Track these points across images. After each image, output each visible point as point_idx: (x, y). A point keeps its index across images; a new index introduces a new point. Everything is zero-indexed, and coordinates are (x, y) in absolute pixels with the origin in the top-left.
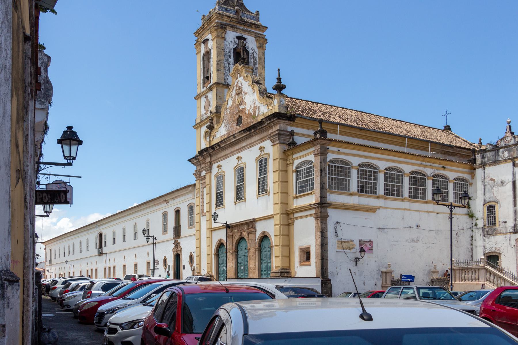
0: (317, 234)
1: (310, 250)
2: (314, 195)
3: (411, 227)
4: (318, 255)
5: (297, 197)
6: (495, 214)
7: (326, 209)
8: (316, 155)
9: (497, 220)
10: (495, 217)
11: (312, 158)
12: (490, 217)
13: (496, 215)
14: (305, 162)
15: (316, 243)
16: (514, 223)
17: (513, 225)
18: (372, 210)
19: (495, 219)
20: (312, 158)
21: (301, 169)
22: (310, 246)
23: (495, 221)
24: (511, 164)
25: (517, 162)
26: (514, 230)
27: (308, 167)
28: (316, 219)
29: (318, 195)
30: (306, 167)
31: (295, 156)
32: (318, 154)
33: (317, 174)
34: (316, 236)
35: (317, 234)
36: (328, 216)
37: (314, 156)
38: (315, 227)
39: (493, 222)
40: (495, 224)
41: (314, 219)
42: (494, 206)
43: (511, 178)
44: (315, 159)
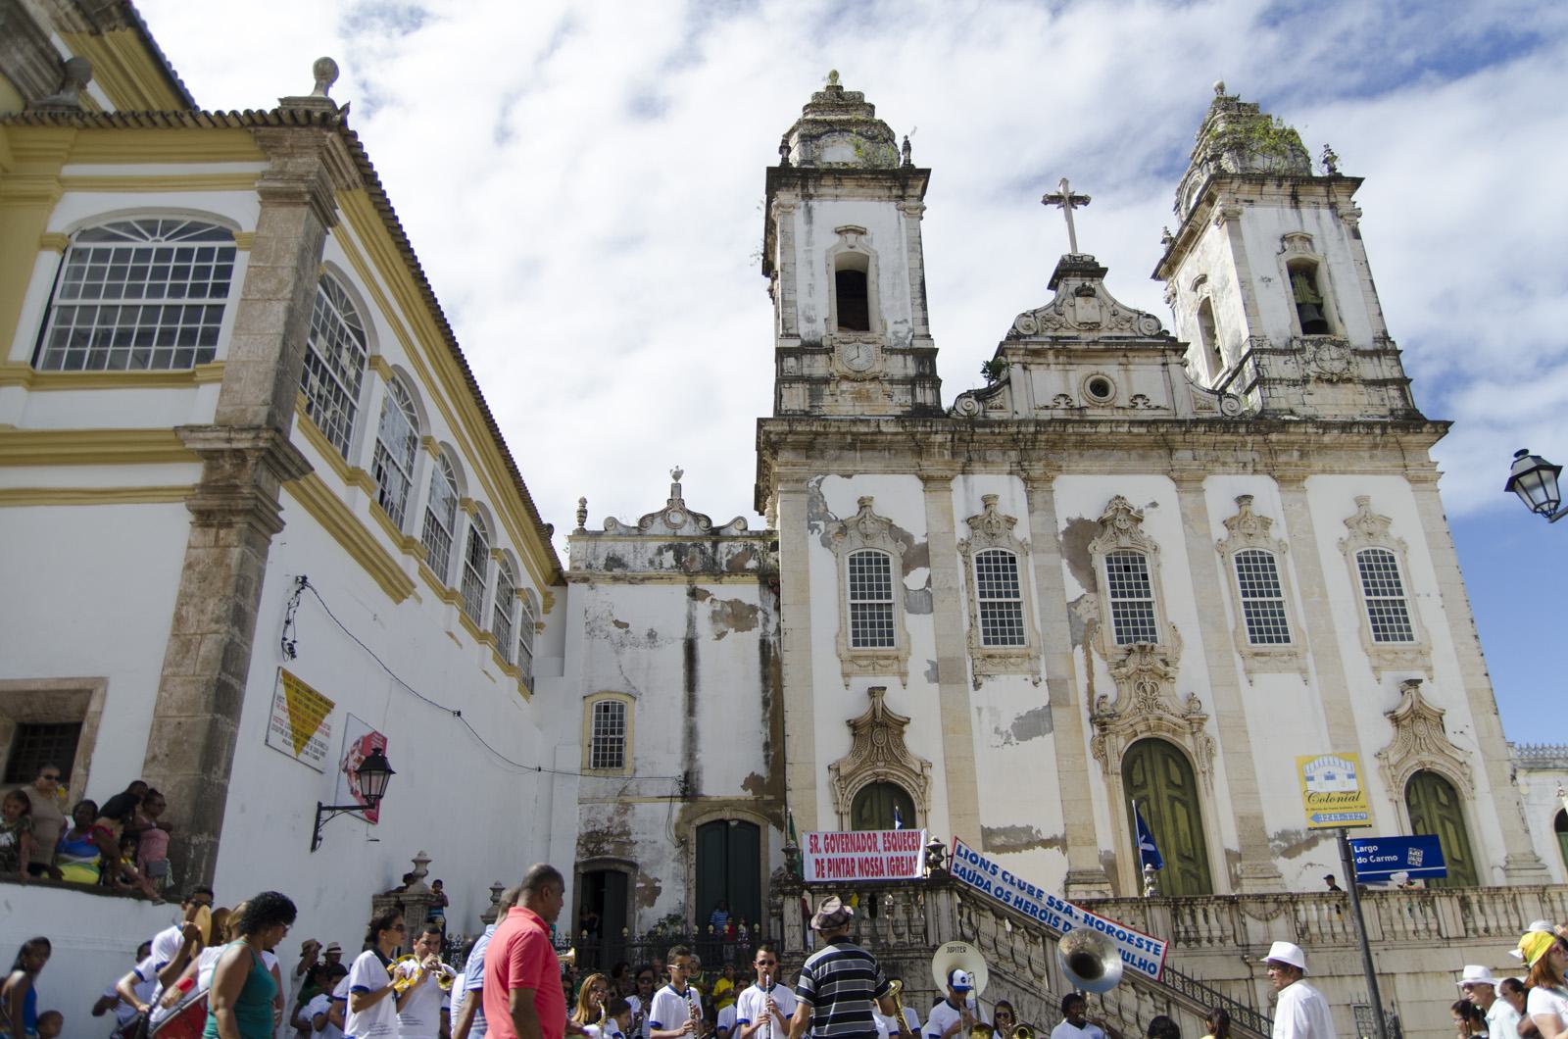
0: (190, 612)
1: (93, 707)
2: (216, 388)
3: (459, 714)
4: (177, 743)
5: (34, 383)
6: (621, 732)
7: (276, 484)
8: (269, 197)
9: (627, 753)
10: (620, 741)
11: (241, 209)
12: (605, 740)
13: (627, 736)
14: (161, 218)
15: (167, 664)
16: (685, 769)
17: (679, 772)
18: (397, 588)
19: (620, 749)
20: (241, 209)
21: (113, 245)
22: (102, 681)
23: (620, 756)
24: (681, 590)
25: (700, 586)
26: (685, 790)
27: (175, 245)
28: (204, 518)
29: (255, 400)
30: (165, 244)
31: (70, 170)
32: (300, 194)
33: (270, 285)
34: (179, 619)
35: (190, 612)
36: (277, 526)
37: (259, 198)
38: (189, 566)
39: (612, 756)
40: (619, 764)
41: (191, 518)
42: (621, 708)
43: (681, 631)
44: (262, 214)
